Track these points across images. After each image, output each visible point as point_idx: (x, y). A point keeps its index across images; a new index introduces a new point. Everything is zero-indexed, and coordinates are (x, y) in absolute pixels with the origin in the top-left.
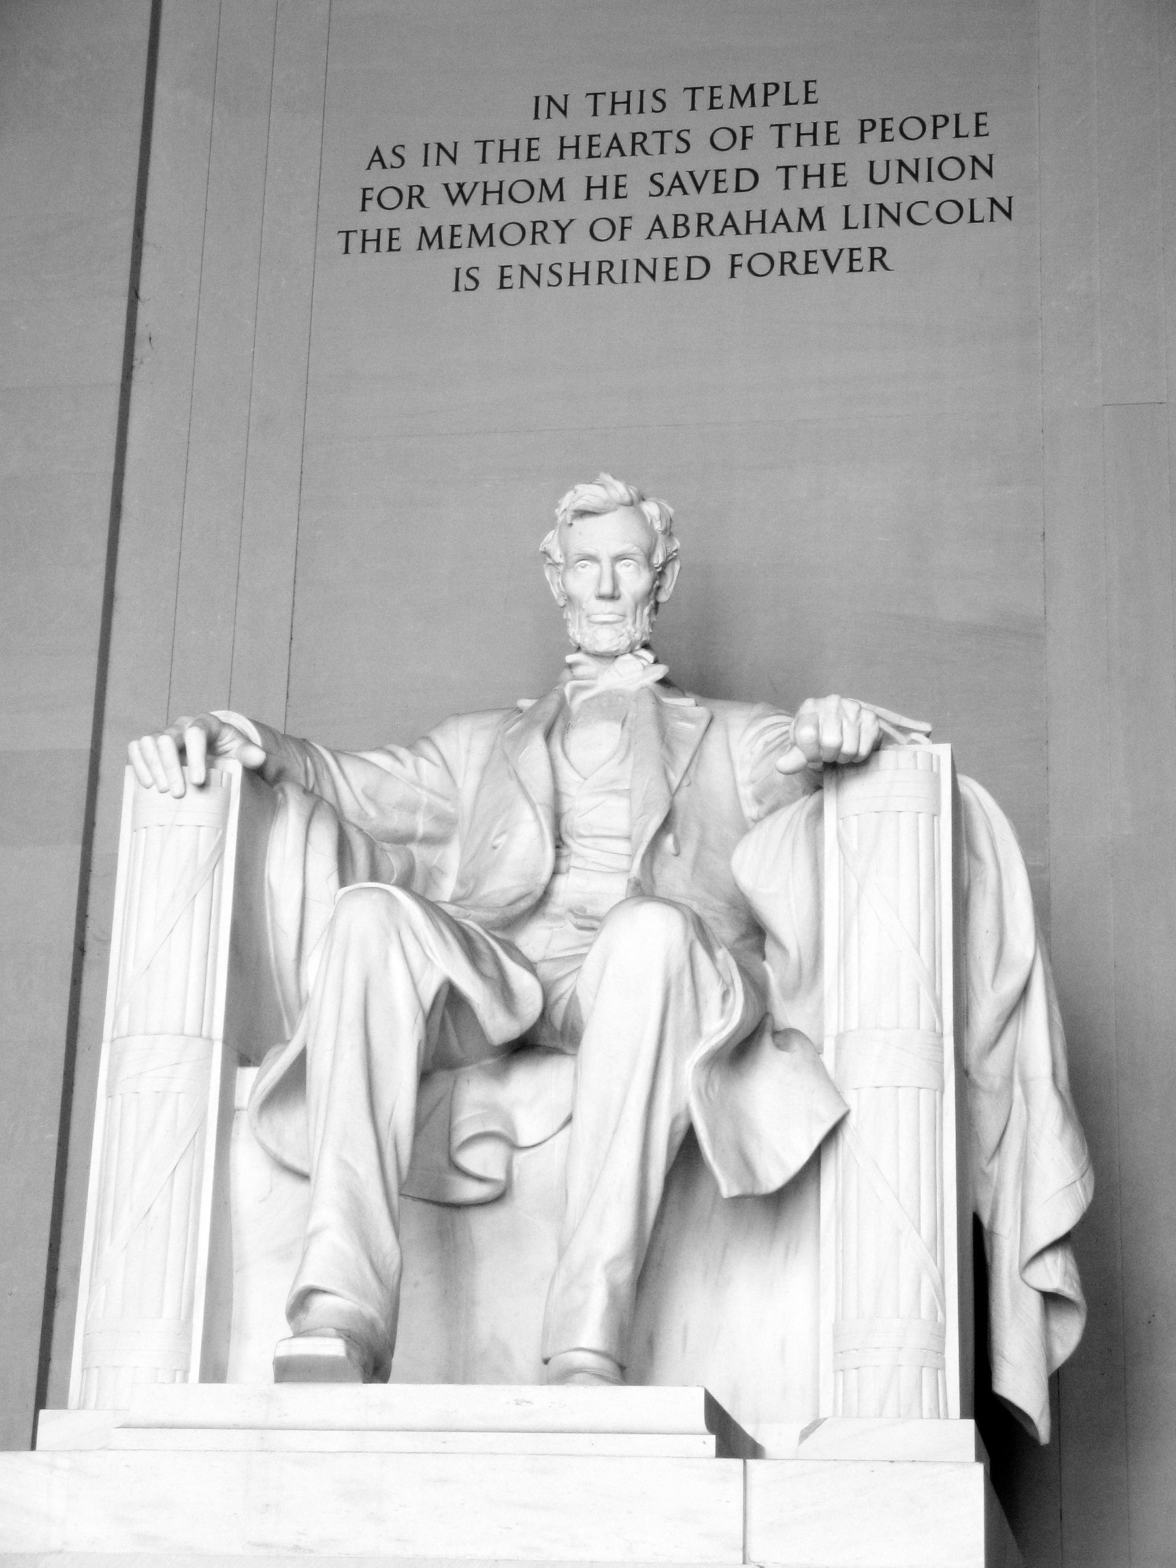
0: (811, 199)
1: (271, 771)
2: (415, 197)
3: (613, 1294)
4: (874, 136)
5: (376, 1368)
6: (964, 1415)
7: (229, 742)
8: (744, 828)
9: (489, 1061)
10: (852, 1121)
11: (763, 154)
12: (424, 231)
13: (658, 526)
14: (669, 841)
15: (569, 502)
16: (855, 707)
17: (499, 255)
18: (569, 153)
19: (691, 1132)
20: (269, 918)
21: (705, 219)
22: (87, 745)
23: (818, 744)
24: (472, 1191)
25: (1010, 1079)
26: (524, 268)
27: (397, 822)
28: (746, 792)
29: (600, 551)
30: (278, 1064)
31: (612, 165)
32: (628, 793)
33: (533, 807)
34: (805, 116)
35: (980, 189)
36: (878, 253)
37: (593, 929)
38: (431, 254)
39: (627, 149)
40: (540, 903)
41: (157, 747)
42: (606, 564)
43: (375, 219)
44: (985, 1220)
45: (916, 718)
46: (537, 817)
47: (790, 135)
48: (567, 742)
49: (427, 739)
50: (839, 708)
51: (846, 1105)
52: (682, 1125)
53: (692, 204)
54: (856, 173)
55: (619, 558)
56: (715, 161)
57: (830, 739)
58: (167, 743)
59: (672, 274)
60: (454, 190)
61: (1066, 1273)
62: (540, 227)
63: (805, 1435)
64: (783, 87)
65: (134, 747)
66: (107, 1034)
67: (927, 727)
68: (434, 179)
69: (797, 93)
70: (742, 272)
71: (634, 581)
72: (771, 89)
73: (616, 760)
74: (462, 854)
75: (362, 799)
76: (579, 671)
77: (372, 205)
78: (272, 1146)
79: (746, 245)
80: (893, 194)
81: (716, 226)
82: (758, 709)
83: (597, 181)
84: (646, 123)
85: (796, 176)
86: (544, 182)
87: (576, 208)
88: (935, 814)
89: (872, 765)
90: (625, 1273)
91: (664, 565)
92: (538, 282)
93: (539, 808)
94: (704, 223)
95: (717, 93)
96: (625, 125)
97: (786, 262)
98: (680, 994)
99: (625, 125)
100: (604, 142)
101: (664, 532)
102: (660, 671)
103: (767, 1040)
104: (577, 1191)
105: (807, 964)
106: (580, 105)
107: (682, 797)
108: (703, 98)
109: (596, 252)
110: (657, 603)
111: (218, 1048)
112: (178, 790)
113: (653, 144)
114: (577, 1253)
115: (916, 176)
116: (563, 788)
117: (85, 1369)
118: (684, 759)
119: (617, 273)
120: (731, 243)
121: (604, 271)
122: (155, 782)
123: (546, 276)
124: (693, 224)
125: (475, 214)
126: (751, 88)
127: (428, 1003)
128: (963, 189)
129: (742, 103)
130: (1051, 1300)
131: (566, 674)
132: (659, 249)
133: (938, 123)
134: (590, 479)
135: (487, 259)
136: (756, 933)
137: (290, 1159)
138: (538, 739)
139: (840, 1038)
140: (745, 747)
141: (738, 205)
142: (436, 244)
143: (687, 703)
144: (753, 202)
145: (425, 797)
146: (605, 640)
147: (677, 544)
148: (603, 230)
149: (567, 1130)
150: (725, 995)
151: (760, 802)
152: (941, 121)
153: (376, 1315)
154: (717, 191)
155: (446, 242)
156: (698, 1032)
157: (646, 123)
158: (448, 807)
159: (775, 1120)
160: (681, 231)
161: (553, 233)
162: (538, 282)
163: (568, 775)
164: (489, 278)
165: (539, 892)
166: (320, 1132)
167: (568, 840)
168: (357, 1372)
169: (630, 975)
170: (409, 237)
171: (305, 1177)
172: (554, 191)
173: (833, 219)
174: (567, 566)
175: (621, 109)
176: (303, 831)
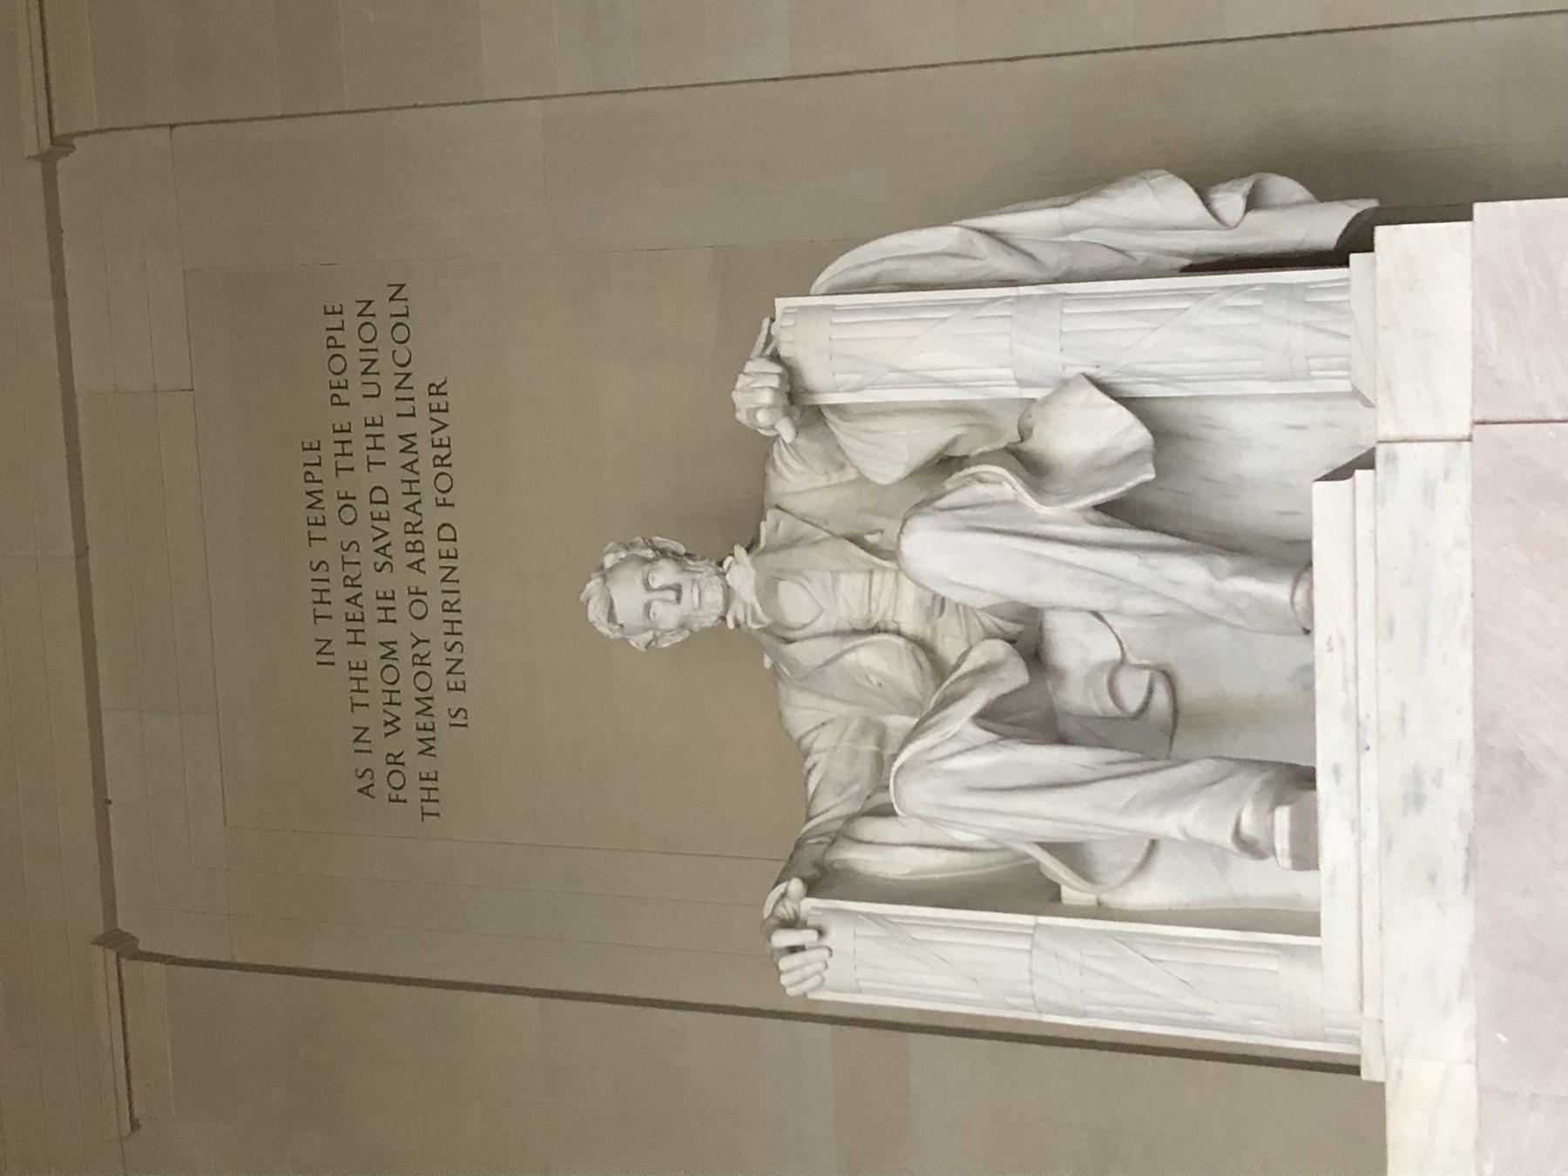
1: (811, 872)
2: (395, 760)
5: (1304, 778)
6: (1346, 264)
7: (786, 911)
8: (862, 480)
9: (1050, 685)
10: (1091, 371)
11: (360, 482)
12: (422, 753)
13: (623, 555)
14: (871, 539)
15: (604, 629)
16: (741, 377)
19: (1098, 508)
20: (937, 876)
21: (409, 528)
22: (828, 1028)
23: (770, 407)
24: (1161, 699)
25: (1063, 244)
26: (449, 672)
27: (865, 768)
28: (835, 478)
29: (643, 601)
30: (1053, 867)
32: (835, 574)
34: (329, 450)
36: (433, 390)
38: (439, 747)
39: (357, 591)
40: (923, 646)
41: (789, 971)
43: (413, 793)
44: (1186, 262)
45: (759, 331)
47: (344, 462)
48: (795, 625)
49: (799, 741)
50: (742, 390)
51: (1077, 376)
52: (1093, 515)
54: (372, 409)
56: (364, 520)
57: (766, 398)
58: (785, 963)
59: (452, 553)
60: (390, 728)
61: (1229, 190)
62: (417, 660)
64: (307, 468)
65: (791, 991)
66: (1034, 1016)
67: (766, 322)
68: (382, 745)
69: (312, 457)
70: (449, 498)
71: (665, 573)
72: (309, 478)
73: (805, 582)
74: (892, 713)
75: (844, 796)
76: (741, 617)
78: (1125, 874)
79: (429, 496)
81: (415, 519)
84: (336, 574)
85: (375, 456)
86: (383, 657)
87: (401, 632)
88: (832, 308)
89: (790, 363)
90: (1223, 562)
91: (654, 549)
92: (460, 661)
93: (846, 647)
95: (312, 521)
96: (339, 594)
97: (441, 462)
98: (977, 518)
99: (339, 594)
100: (351, 609)
101: (627, 549)
102: (740, 551)
105: (970, 419)
106: (325, 629)
107: (839, 530)
110: (687, 555)
111: (1044, 920)
112: (826, 953)
113: (352, 571)
114: (1207, 604)
115: (374, 361)
116: (831, 629)
117: (1325, 1039)
119: (452, 598)
120: (427, 506)
122: (819, 973)
123: (455, 654)
124: (412, 538)
125: (408, 711)
126: (310, 494)
127: (991, 736)
128: (383, 323)
129: (320, 501)
132: (432, 565)
134: (584, 608)
135: (443, 702)
136: (945, 464)
137: (1137, 859)
139: (1022, 383)
140: (798, 479)
141: (399, 501)
142: (431, 743)
144: (396, 490)
146: (714, 596)
147: (638, 539)
148: (419, 610)
149: (1106, 616)
150: (981, 481)
151: (842, 466)
152: (331, 342)
153: (1259, 779)
154: (387, 519)
155: (431, 735)
156: (1014, 503)
157: (336, 574)
158: (856, 723)
159: (1090, 432)
160: (419, 547)
161: (422, 649)
162: (460, 661)
163: (821, 625)
164: (456, 701)
165: (911, 646)
166: (1100, 830)
167: (874, 622)
168: (1307, 795)
169: (959, 562)
170: (426, 765)
171: (1154, 844)
173: (408, 426)
174: (655, 629)
175: (326, 597)
176: (863, 847)
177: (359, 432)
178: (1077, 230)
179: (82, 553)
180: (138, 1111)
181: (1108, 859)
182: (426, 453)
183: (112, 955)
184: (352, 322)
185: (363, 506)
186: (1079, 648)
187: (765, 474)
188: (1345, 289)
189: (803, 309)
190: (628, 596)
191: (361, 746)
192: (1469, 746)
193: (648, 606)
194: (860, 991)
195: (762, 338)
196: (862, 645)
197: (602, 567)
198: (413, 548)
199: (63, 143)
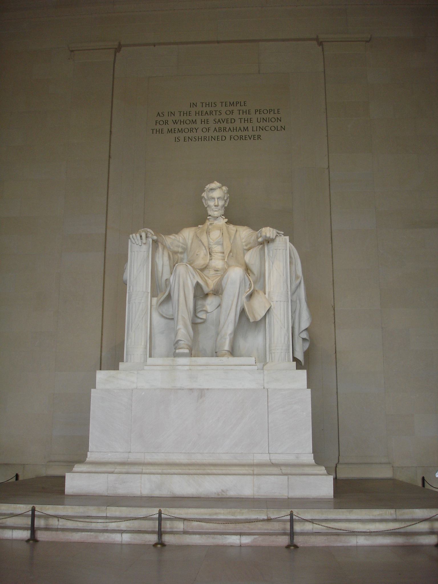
0: (246, 125)
2: (166, 122)
3: (230, 340)
10: (272, 307)
11: (236, 116)
15: (207, 186)
18: (197, 114)
22: (105, 232)
23: (266, 236)
24: (199, 321)
27: (176, 249)
28: (244, 244)
31: (206, 117)
33: (205, 247)
34: (244, 108)
35: (278, 124)
37: (217, 271)
42: (216, 200)
43: (158, 127)
45: (280, 231)
46: (206, 249)
47: (241, 112)
53: (222, 125)
54: (254, 120)
57: (268, 235)
60: (174, 121)
63: (264, 365)
65: (131, 236)
66: (128, 292)
69: (242, 104)
70: (232, 139)
71: (221, 203)
77: (158, 124)
78: (161, 312)
81: (227, 130)
82: (245, 227)
83: (203, 120)
85: (243, 121)
87: (199, 125)
88: (286, 250)
90: (232, 335)
94: (225, 129)
96: (208, 109)
97: (241, 138)
99: (208, 109)
102: (226, 220)
103: (256, 292)
104: (222, 321)
108: (224, 104)
109: (203, 135)
111: (150, 294)
113: (214, 113)
118: (232, 237)
119: (207, 139)
120: (230, 133)
123: (193, 139)
124: (222, 129)
128: (275, 124)
130: (304, 339)
131: (207, 221)
132: (216, 134)
133: (270, 111)
134: (212, 182)
135: (182, 135)
137: (164, 315)
138: (205, 233)
139: (269, 293)
141: (231, 126)
143: (231, 226)
145: (181, 245)
148: (204, 130)
151: (246, 246)
155: (173, 132)
161: (194, 130)
164: (182, 139)
170: (165, 130)
172: (195, 122)
173: (250, 129)
177: (249, 116)
178: (300, 304)
181: (167, 309)
182: (244, 133)
183: (117, 47)
184: (276, 116)
185: (230, 117)
186: (210, 303)
187: (244, 226)
188: (289, 361)
189: (286, 243)
191: (170, 113)
192: (202, 387)
194: (131, 252)
195: (279, 232)
196: (207, 252)
197: (223, 186)
198: (220, 129)
199: (321, 44)
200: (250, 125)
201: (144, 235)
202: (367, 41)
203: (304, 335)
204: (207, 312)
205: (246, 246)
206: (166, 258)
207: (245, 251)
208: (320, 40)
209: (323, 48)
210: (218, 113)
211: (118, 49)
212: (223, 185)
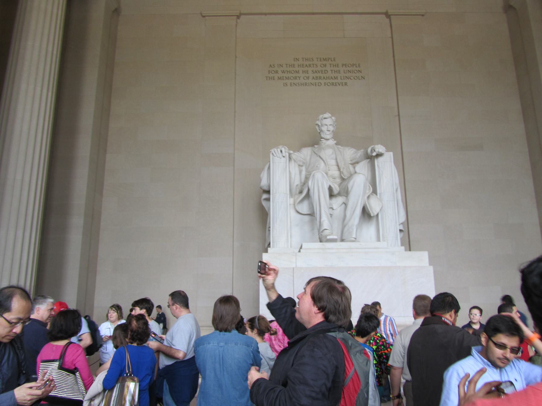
0: (336, 75)
4: (344, 66)
11: (328, 68)
15: (321, 116)
17: (290, 81)
31: (306, 69)
34: (334, 63)
43: (271, 75)
53: (318, 75)
55: (330, 125)
58: (279, 150)
69: (333, 60)
71: (331, 128)
80: (348, 75)
84: (311, 63)
87: (301, 75)
96: (308, 63)
97: (333, 84)
99: (308, 63)
100: (305, 65)
102: (335, 142)
109: (304, 81)
113: (312, 66)
120: (324, 81)
121: (306, 84)
128: (357, 75)
130: (401, 231)
132: (314, 81)
133: (353, 65)
137: (300, 211)
141: (325, 75)
143: (340, 146)
146: (328, 137)
151: (351, 161)
157: (311, 63)
164: (289, 84)
170: (276, 78)
172: (297, 72)
173: (339, 78)
179: (313, 14)
180: (207, 18)
182: (334, 81)
183: (238, 14)
184: (358, 69)
185: (324, 69)
186: (337, 202)
190: (328, 122)
193: (326, 125)
194: (273, 163)
198: (317, 77)
200: (339, 75)
201: (283, 150)
202: (423, 15)
203: (402, 228)
204: (332, 208)
205: (351, 161)
206: (297, 168)
207: (350, 166)
208: (390, 14)
209: (390, 21)
210: (315, 66)
211: (238, 17)
212: (332, 116)
